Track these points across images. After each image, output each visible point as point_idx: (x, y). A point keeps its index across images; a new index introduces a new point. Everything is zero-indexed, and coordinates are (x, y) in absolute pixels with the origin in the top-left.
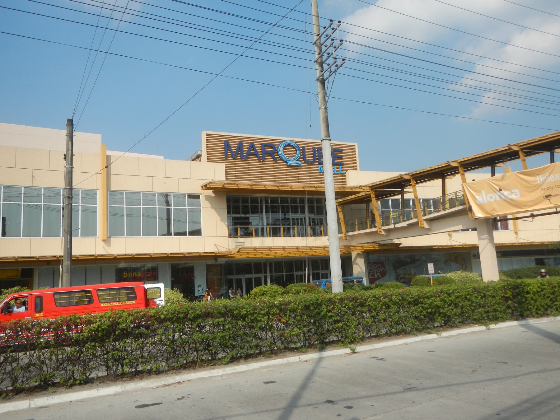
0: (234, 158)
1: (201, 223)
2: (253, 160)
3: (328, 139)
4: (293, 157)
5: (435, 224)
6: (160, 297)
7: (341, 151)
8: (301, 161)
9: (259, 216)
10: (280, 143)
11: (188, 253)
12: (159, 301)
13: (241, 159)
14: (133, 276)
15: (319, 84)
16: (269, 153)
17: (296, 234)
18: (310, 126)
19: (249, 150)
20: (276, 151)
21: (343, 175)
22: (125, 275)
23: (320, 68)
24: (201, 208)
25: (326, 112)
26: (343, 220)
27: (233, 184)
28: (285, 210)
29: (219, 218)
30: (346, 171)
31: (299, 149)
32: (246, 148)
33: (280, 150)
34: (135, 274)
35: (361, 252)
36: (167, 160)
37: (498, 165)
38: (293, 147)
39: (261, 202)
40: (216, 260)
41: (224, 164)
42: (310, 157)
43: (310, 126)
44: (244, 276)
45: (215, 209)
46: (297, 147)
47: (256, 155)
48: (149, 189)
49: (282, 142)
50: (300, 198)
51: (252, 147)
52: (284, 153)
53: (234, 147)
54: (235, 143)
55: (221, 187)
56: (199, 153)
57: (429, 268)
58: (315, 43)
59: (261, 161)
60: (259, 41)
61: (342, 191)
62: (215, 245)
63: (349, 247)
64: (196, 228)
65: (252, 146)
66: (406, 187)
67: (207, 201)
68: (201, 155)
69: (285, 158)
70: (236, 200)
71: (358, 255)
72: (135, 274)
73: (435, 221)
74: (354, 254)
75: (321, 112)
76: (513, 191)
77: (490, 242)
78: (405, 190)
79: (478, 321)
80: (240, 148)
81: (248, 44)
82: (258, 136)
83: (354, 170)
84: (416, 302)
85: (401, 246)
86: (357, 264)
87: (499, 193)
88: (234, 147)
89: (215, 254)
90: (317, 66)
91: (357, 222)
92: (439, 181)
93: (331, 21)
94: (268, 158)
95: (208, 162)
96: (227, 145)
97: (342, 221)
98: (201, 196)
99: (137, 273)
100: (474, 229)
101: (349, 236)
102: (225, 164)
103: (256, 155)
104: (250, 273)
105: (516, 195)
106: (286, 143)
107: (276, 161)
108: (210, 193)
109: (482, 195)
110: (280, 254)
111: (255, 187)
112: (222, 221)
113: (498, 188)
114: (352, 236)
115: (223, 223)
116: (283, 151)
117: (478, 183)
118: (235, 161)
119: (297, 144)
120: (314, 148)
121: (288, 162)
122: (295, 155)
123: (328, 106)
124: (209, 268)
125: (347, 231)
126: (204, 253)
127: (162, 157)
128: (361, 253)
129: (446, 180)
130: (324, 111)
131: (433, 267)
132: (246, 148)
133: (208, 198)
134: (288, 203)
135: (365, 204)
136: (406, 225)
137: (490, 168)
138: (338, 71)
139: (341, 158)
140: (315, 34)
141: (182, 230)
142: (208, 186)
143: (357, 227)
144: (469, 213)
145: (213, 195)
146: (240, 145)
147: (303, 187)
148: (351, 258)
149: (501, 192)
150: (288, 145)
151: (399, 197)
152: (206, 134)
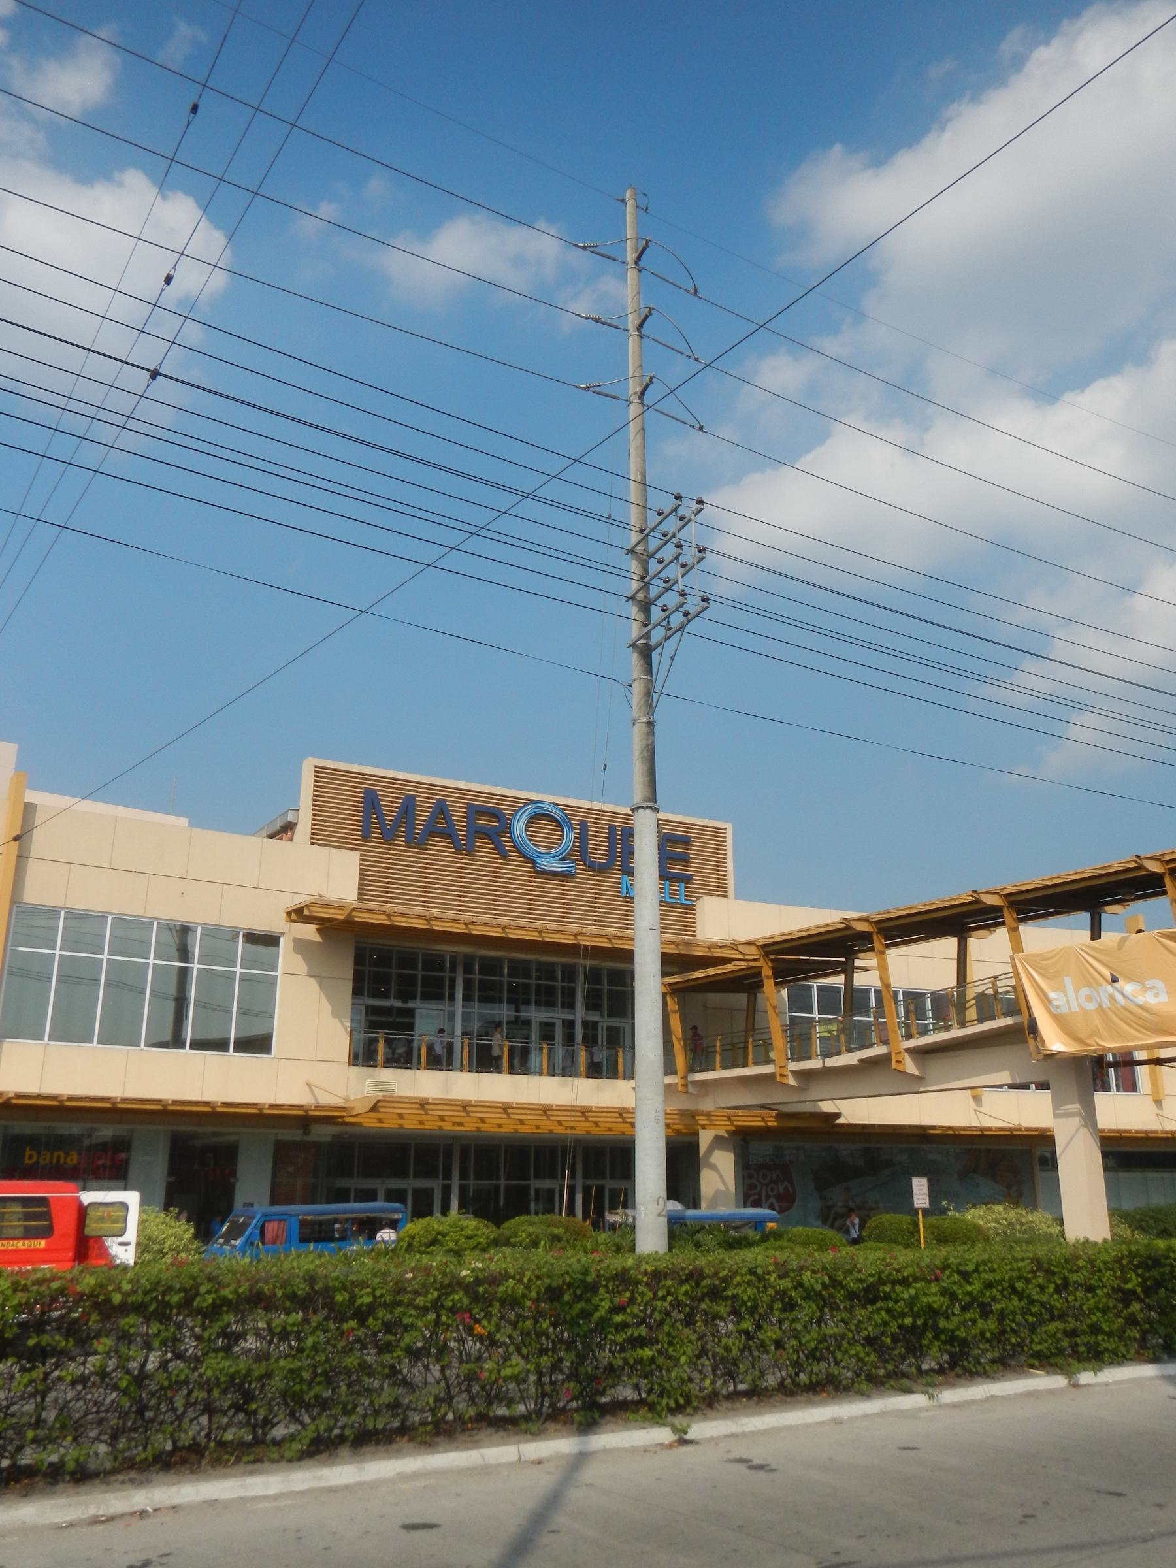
0: (388, 840)
1: (273, 1017)
2: (439, 849)
3: (650, 808)
4: (553, 848)
5: (937, 1066)
6: (123, 1232)
7: (685, 841)
8: (573, 861)
10: (520, 808)
11: (225, 1104)
12: (121, 1244)
13: (408, 844)
14: (55, 1161)
15: (635, 658)
16: (485, 834)
17: (544, 1067)
18: (605, 768)
19: (433, 819)
20: (506, 829)
21: (689, 908)
22: (31, 1157)
23: (641, 617)
24: (279, 974)
25: (651, 733)
26: (680, 1035)
27: (377, 913)
28: (518, 998)
29: (327, 1007)
30: (698, 898)
31: (571, 828)
32: (422, 814)
33: (519, 827)
34: (59, 1158)
35: (727, 1131)
36: (197, 831)
37: (1108, 909)
38: (555, 820)
39: (453, 969)
40: (306, 1132)
42: (598, 853)
43: (605, 768)
44: (383, 1182)
45: (320, 979)
46: (564, 821)
47: (449, 834)
48: (134, 908)
49: (526, 804)
50: (564, 966)
51: (442, 812)
52: (528, 835)
53: (390, 807)
54: (393, 797)
55: (342, 917)
56: (291, 817)
57: (915, 1189)
58: (631, 551)
59: (462, 854)
60: (482, 532)
61: (683, 952)
62: (309, 1085)
63: (693, 1117)
64: (256, 1030)
65: (441, 810)
66: (860, 955)
67: (299, 957)
68: (295, 824)
69: (530, 849)
70: (384, 958)
71: (718, 1142)
72: (59, 1158)
73: (940, 1055)
74: (705, 1138)
75: (638, 732)
76: (1149, 983)
77: (1086, 1126)
78: (857, 962)
79: (1046, 1361)
80: (406, 813)
81: (452, 538)
82: (461, 785)
83: (718, 896)
84: (870, 1295)
85: (838, 1122)
86: (714, 1168)
87: (1109, 988)
88: (390, 807)
89: (306, 1111)
90: (634, 611)
91: (718, 1044)
92: (949, 945)
93: (678, 497)
94: (482, 845)
95: (312, 844)
96: (371, 802)
97: (679, 1040)
98: (282, 940)
99: (67, 1154)
100: (1043, 1086)
101: (694, 1083)
102: (361, 855)
103: (449, 836)
104: (402, 1173)
105: (1156, 995)
106: (536, 808)
107: (503, 855)
108: (309, 932)
109: (1065, 992)
110: (494, 1125)
111: (438, 926)
112: (335, 1014)
113: (1107, 973)
114: (704, 1084)
115: (336, 1021)
116: (527, 831)
117: (1055, 955)
118: (390, 849)
119: (566, 815)
120: (612, 829)
121: (538, 861)
123: (658, 716)
124: (283, 1153)
125: (692, 1069)
126: (273, 1106)
127: (184, 822)
128: (725, 1134)
129: (970, 941)
130: (644, 729)
131: (925, 1190)
132: (422, 814)
133: (301, 946)
134: (528, 977)
135: (746, 995)
136: (855, 1062)
137: (1086, 917)
138: (690, 628)
139: (685, 860)
140: (633, 528)
141: (214, 1035)
142: (306, 912)
143: (718, 1058)
144: (1030, 1039)
145: (317, 938)
146: (408, 807)
147: (575, 936)
148: (695, 1146)
149: (1115, 984)
150: (541, 816)
151: (838, 980)
152: (316, 767)
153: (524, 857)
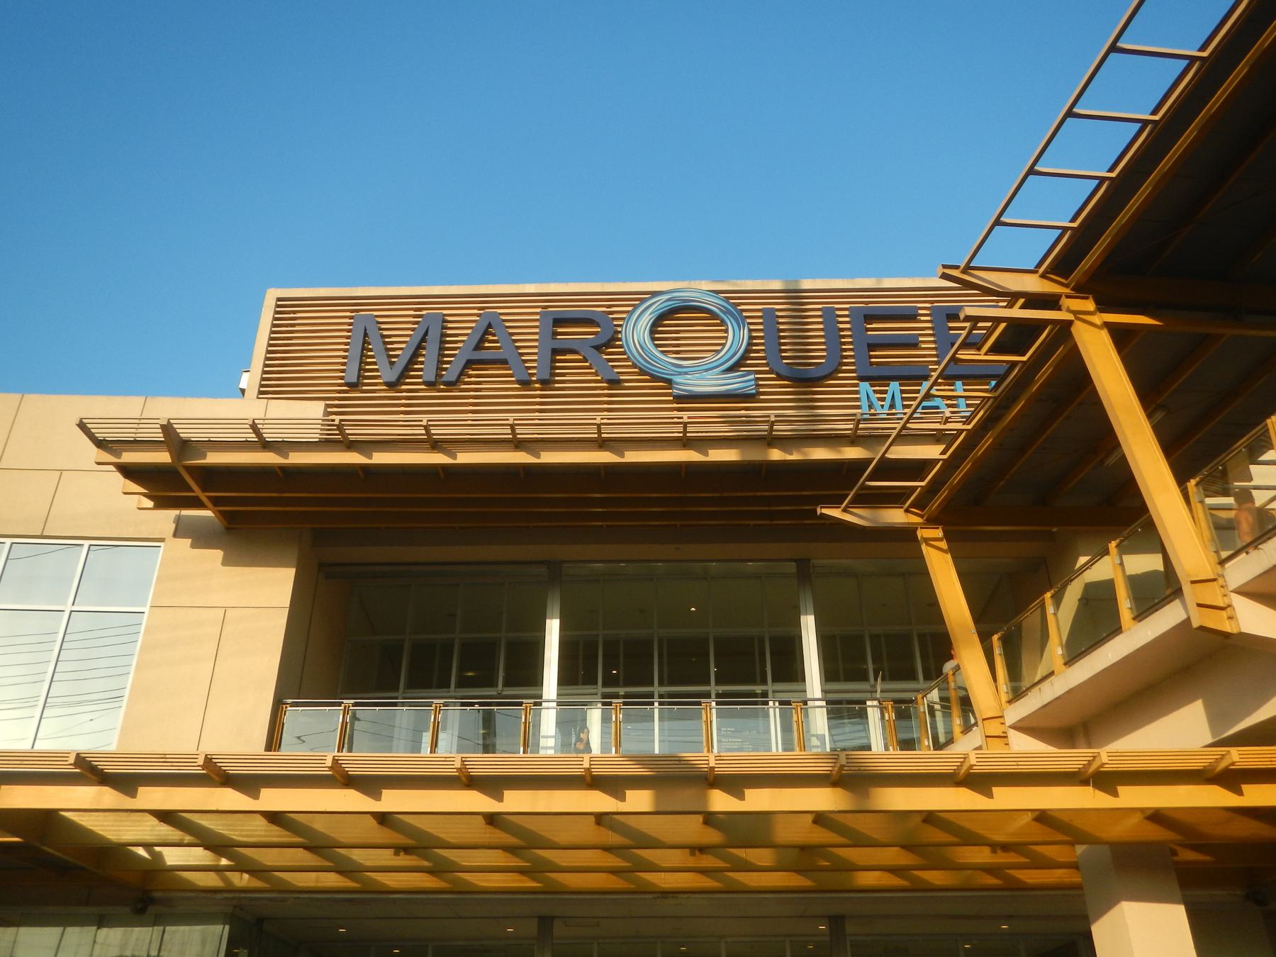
9: (595, 691)
10: (643, 301)
20: (611, 341)
31: (741, 319)
33: (637, 332)
38: (713, 315)
41: (321, 404)
46: (727, 312)
52: (653, 339)
53: (402, 341)
59: (536, 389)
69: (664, 362)
121: (677, 379)
122: (718, 352)
152: (279, 299)
153: (655, 378)
